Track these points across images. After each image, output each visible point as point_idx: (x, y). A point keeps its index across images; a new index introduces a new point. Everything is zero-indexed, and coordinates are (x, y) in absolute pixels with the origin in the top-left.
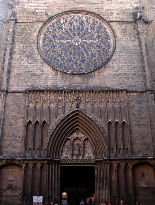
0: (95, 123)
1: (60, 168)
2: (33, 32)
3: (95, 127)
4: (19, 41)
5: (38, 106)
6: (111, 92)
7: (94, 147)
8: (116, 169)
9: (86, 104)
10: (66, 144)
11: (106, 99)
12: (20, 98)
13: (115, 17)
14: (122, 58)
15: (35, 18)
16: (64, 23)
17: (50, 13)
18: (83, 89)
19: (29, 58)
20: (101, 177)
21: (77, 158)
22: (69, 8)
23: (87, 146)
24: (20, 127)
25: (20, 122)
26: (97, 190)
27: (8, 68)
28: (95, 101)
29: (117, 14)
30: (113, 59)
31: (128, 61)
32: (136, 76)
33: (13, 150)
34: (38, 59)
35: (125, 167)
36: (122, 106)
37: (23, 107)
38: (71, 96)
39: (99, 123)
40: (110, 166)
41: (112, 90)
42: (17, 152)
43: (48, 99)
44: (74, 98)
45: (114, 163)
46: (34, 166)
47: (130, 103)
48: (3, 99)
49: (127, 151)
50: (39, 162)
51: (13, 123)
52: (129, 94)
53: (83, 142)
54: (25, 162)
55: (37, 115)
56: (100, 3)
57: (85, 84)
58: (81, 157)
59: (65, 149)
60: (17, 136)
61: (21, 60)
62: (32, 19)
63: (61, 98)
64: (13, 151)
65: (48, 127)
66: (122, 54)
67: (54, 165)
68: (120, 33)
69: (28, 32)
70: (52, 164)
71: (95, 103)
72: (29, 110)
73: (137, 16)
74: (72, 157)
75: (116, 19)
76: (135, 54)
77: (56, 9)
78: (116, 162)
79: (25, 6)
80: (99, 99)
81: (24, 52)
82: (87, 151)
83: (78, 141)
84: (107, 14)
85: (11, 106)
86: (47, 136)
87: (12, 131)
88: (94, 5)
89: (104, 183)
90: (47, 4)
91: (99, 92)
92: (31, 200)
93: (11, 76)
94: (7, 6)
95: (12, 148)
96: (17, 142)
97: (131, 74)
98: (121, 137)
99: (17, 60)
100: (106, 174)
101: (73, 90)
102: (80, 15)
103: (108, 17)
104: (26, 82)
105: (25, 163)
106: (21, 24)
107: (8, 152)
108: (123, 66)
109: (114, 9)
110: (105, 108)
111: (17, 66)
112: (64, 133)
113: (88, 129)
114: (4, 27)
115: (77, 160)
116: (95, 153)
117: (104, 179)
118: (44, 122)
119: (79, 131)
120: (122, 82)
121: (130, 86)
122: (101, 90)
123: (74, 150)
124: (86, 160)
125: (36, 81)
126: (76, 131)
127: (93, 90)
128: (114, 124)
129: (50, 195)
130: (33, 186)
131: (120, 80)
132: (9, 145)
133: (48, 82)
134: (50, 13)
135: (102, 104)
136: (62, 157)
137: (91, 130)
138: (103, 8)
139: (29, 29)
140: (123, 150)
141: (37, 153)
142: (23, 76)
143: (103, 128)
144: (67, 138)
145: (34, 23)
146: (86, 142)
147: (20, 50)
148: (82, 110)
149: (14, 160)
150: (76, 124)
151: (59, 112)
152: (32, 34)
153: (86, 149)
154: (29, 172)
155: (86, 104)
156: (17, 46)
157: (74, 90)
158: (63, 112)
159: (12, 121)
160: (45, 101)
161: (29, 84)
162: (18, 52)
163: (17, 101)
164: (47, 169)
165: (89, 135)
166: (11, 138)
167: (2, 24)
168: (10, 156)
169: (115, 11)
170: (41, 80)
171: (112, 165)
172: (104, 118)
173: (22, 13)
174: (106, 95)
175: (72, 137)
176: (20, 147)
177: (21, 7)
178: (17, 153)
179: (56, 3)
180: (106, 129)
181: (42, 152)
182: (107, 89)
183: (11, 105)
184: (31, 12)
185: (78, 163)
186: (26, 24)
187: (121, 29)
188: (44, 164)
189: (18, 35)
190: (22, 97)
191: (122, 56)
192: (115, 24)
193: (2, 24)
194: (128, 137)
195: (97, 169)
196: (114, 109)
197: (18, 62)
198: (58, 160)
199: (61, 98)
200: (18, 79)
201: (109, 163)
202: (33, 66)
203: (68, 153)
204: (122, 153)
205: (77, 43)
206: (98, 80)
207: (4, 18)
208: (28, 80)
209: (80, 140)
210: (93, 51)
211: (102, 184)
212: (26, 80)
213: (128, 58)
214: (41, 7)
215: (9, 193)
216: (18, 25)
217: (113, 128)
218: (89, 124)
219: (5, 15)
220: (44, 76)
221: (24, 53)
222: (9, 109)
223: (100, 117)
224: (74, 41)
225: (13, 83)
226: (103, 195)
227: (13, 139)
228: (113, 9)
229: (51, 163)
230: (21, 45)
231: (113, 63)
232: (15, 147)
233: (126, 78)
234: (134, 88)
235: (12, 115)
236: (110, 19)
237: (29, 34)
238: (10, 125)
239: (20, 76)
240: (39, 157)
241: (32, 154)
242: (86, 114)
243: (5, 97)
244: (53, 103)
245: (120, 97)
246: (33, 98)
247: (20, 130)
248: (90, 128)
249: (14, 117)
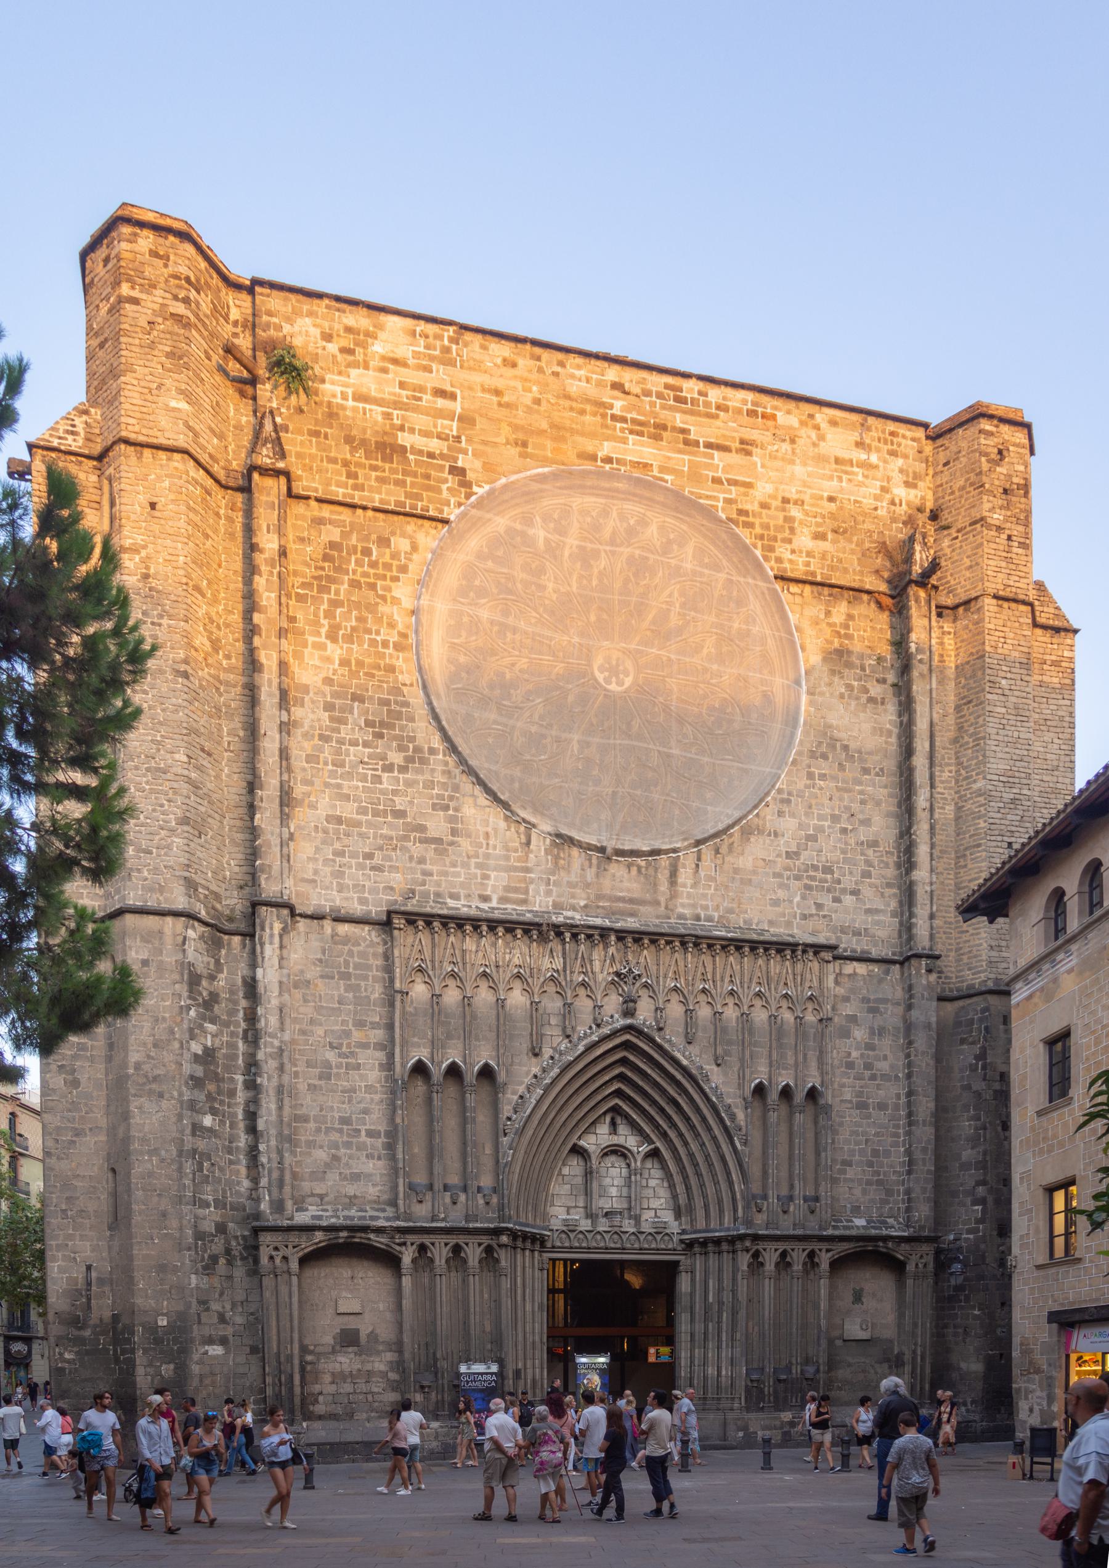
5: (452, 996)
12: (361, 948)
18: (652, 929)
28: (704, 991)
36: (810, 1018)
51: (339, 1066)
73: (909, 559)
80: (722, 980)
87: (337, 1107)
102: (633, 508)
127: (697, 937)
135: (731, 1005)
138: (749, 485)
159: (331, 1056)
161: (397, 880)
182: (755, 937)
183: (319, 982)
215: (346, 1361)
223: (718, 1065)
238: (326, 1076)
248: (670, 1110)
249: (340, 1037)
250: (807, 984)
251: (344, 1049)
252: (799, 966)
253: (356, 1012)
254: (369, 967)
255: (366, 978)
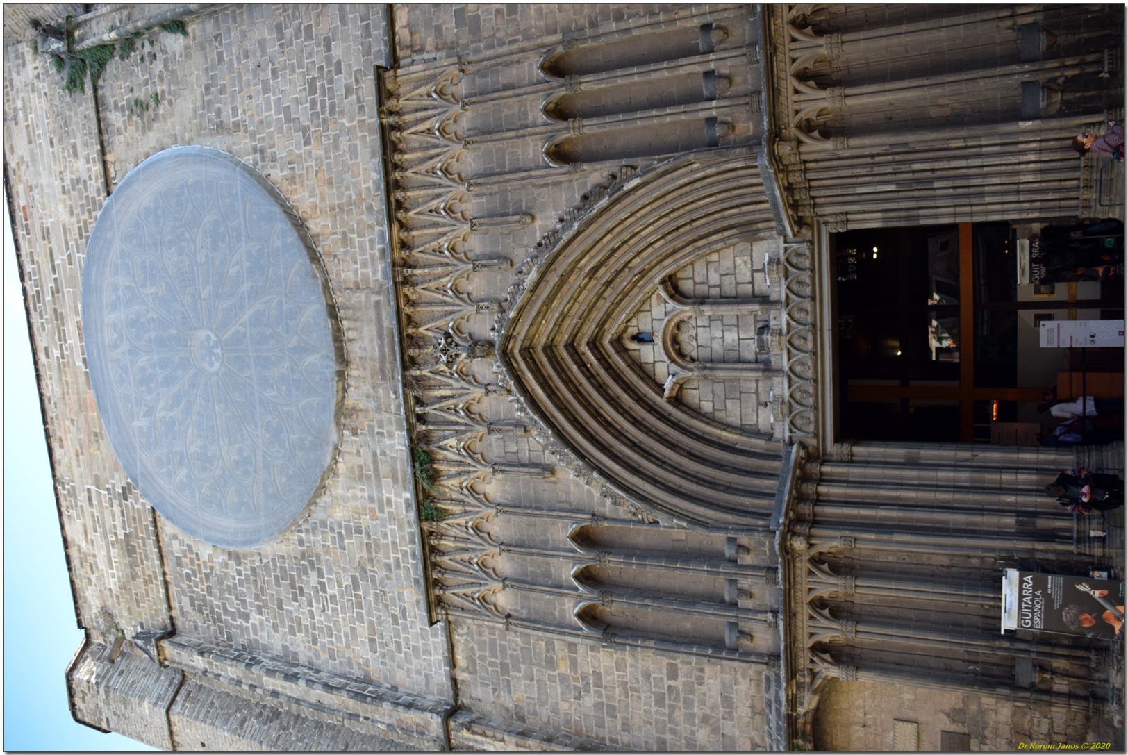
0: (561, 243)
1: (845, 449)
2: (199, 560)
3: (590, 242)
4: (240, 627)
5: (503, 564)
6: (397, 157)
7: (714, 238)
8: (838, 91)
9: (471, 300)
10: (707, 407)
11: (435, 185)
12: (475, 646)
13: (87, 167)
14: (244, 112)
15: (144, 545)
16: (150, 412)
17: (117, 475)
19: (301, 589)
20: (892, 187)
21: (784, 340)
22: (90, 389)
23: (714, 278)
24: (620, 666)
25: (596, 664)
26: (987, 213)
27: (344, 693)
28: (452, 249)
29: (76, 155)
30: (256, 164)
31: (254, 78)
32: (318, 24)
33: (743, 710)
34: (301, 542)
35: (819, 32)
36: (462, 88)
37: (518, 639)
38: (441, 386)
39: (561, 220)
40: (816, 134)
41: (384, 152)
42: (753, 691)
43: (466, 512)
44: (443, 367)
45: (797, 112)
46: (826, 612)
47: (448, 41)
48: (484, 735)
49: (719, 28)
50: (803, 582)
52: (400, 53)
53: (686, 308)
54: (804, 660)
55: (549, 576)
56: (50, 242)
57: (377, 304)
58: (780, 319)
59: (733, 412)
60: (667, 683)
61: (314, 627)
62: (153, 560)
63: (452, 442)
64: (749, 710)
65: (605, 518)
66: (227, 112)
67: (823, 489)
68: (144, 130)
69: (201, 579)
70: (819, 500)
71: (459, 248)
72: (524, 614)
74: (780, 371)
75: (93, 159)
76: (221, 43)
77: (99, 449)
78: (788, 100)
79: (112, 587)
80: (437, 225)
81: (280, 603)
82: (739, 280)
83: (683, 337)
84: (82, 206)
85: (519, 700)
86: (654, 529)
88: (59, 274)
89: (933, 170)
90: (89, 491)
91: (402, 226)
92: (1047, 649)
93: (385, 678)
94: (121, 663)
95: (729, 715)
96: (696, 686)
97: (311, 54)
98: (636, 78)
99: (315, 642)
100: (872, 156)
101: (404, 377)
102: (109, 336)
103: (93, 198)
104: (404, 611)
105: (812, 661)
106: (178, 612)
107: (752, 740)
108: (278, 101)
109: (61, 172)
110: (484, 189)
111: (340, 645)
112: (636, 422)
113: (608, 283)
114: (201, 687)
115: (796, 342)
116: (749, 232)
117: (904, 168)
118: (584, 538)
119: (632, 331)
120: (354, 97)
121: (369, 54)
122: (391, 219)
123: (739, 360)
124: (795, 287)
125: (392, 561)
126: (632, 346)
127: (394, 265)
128: (563, 124)
129: (1010, 521)
130: (953, 626)
131: (342, 112)
132: (715, 730)
133: (389, 501)
134: (117, 475)
136: (782, 431)
137: (615, 263)
138: (64, 226)
139: (188, 577)
140: (712, 56)
141: (755, 590)
142: (380, 624)
143: (585, 198)
144: (670, 401)
145: (164, 554)
146: (687, 286)
147: (275, 627)
148: (499, 321)
149: (791, 720)
150: (589, 353)
151: (525, 456)
152: (204, 562)
153: (729, 289)
154: (867, 637)
155: (471, 300)
156: (263, 638)
157: (404, 368)
158: (521, 432)
159: (589, 701)
160: (477, 529)
162: (285, 633)
163: (492, 664)
164: (845, 538)
165: (643, 273)
166: (679, 715)
167: (189, 692)
168: (775, 736)
169: (65, 167)
170: (385, 536)
171: (808, 120)
172: (536, 192)
173: (137, 601)
174: (413, 188)
175: (665, 372)
176: (722, 672)
177: (119, 604)
178: (759, 691)
179: (81, 447)
180: (596, 174)
181: (748, 559)
184: (127, 560)
185: (810, 337)
186: (173, 589)
187: (129, 128)
188: (814, 552)
189: (220, 628)
190: (473, 639)
191: (235, 110)
192: (114, 163)
193: (188, 696)
194: (628, 30)
195: (847, 213)
196: (484, 133)
197: (326, 640)
198: (793, 456)
199: (452, 442)
200: (393, 647)
201: (800, 142)
202: (330, 571)
203: (757, 393)
204: (728, 63)
205: (215, 351)
206: (355, 236)
207: (166, 684)
208: (394, 598)
209: (678, 326)
210: (237, 268)
211: (936, 185)
212: (398, 613)
213: (240, 80)
214: (102, 513)
216: (183, 623)
217: (586, 130)
218: (576, 280)
219: (157, 675)
220: (366, 521)
221: (282, 609)
222: (535, 711)
223: (533, 218)
224: (211, 365)
225: (414, 675)
226: (1018, 173)
227: (681, 704)
228: (62, 180)
229: (806, 509)
230: (255, 618)
231: (274, 159)
232: (728, 702)
233: (331, 81)
234: (377, 28)
235: (563, 700)
236: (99, 194)
237: (207, 576)
238: (612, 711)
239: (382, 637)
240: (776, 583)
241: (760, 616)
242: (520, 300)
243: (476, 728)
244: (480, 487)
245: (414, 104)
246: (468, 591)
247: (632, 666)
248: (604, 274)
249: (568, 687)
250: (425, 103)
251: (580, 685)
252: (408, 118)
253: (539, 665)
254: (493, 642)
255: (503, 648)
